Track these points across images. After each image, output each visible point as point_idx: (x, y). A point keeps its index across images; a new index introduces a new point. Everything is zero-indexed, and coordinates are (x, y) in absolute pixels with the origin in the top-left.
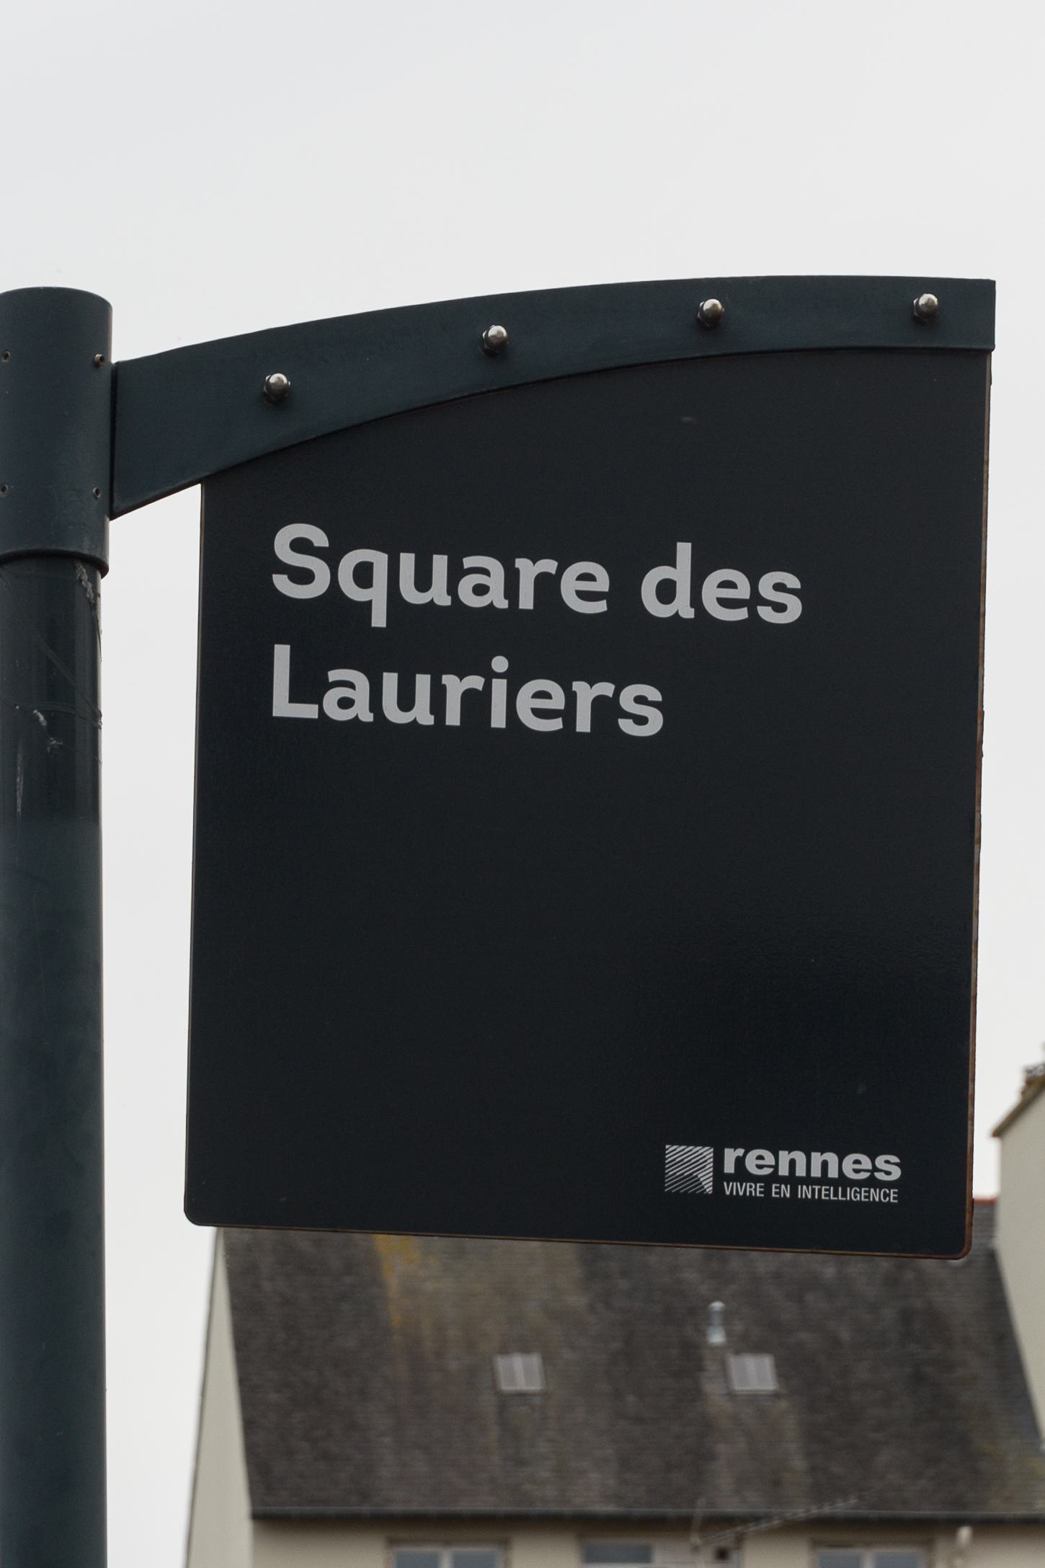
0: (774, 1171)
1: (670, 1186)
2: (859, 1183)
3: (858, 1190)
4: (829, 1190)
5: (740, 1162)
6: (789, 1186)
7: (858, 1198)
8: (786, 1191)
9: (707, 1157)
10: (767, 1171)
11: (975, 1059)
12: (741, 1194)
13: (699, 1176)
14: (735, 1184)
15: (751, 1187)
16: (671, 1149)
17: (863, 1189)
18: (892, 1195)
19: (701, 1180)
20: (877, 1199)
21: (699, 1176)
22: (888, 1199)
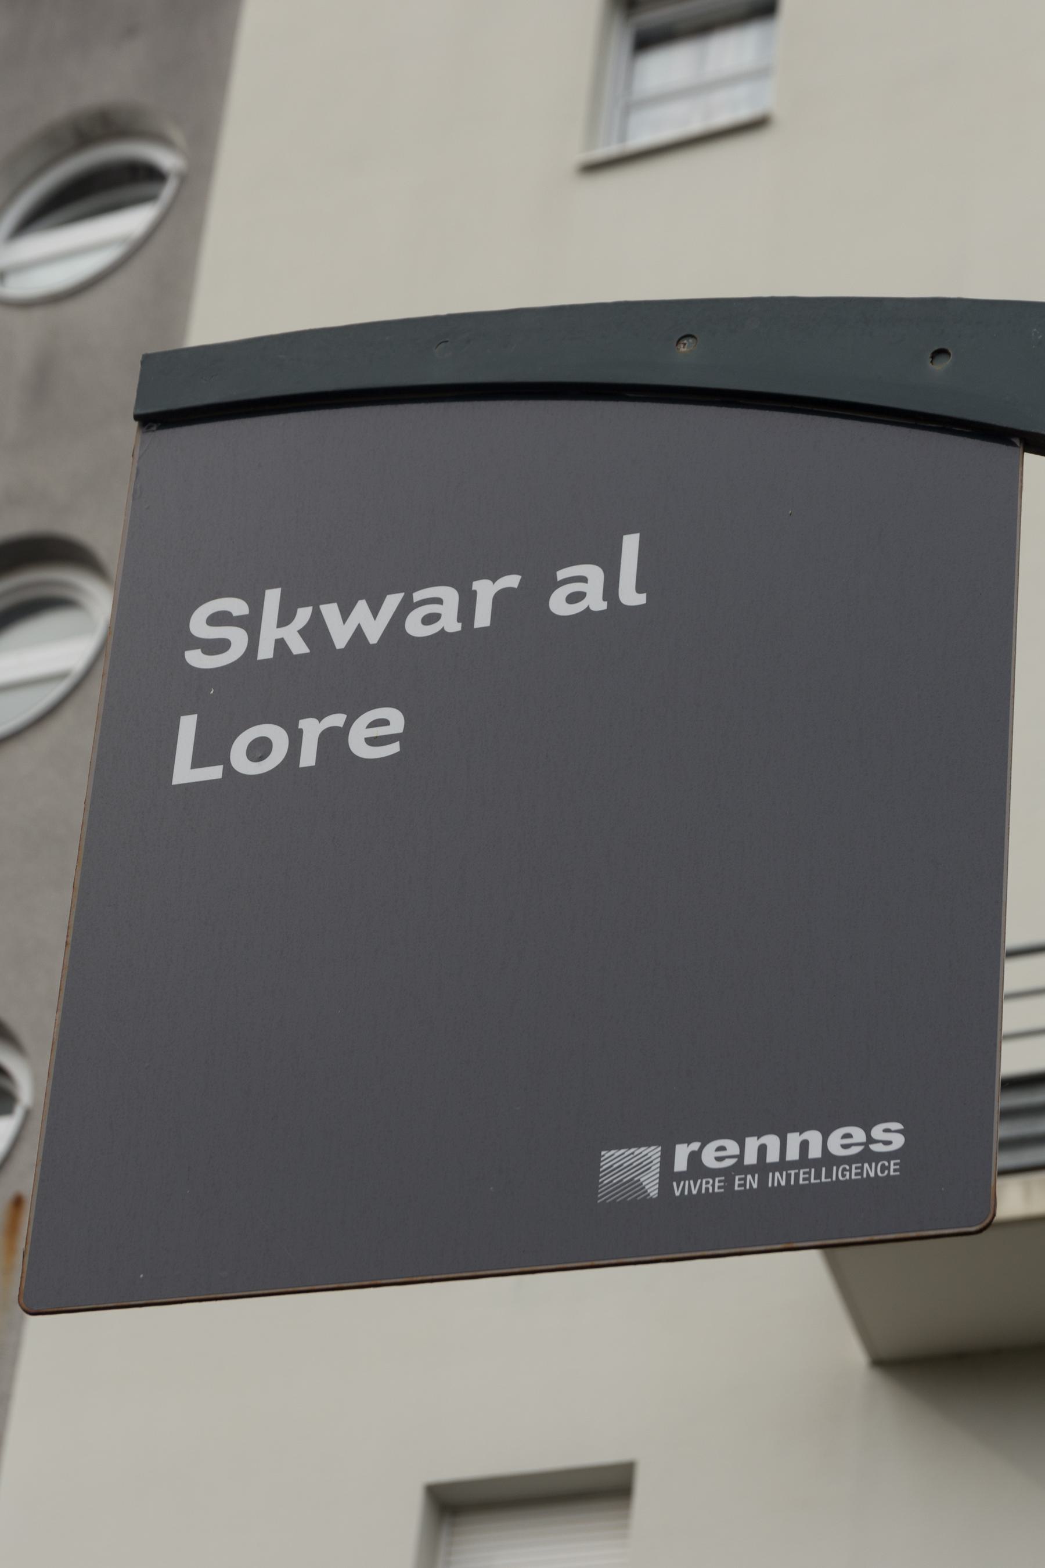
0: (738, 1161)
1: (602, 1197)
2: (849, 1160)
3: (848, 1167)
4: (809, 1173)
5: (695, 1158)
6: (756, 1176)
7: (848, 1177)
8: (753, 1182)
9: (653, 1158)
10: (728, 1163)
11: (1009, 831)
12: (694, 1192)
13: (642, 1180)
14: (687, 1182)
15: (707, 1183)
16: (607, 1156)
17: (854, 1166)
18: (892, 1167)
19: (644, 1184)
20: (872, 1175)
21: (642, 1180)
22: (886, 1172)
